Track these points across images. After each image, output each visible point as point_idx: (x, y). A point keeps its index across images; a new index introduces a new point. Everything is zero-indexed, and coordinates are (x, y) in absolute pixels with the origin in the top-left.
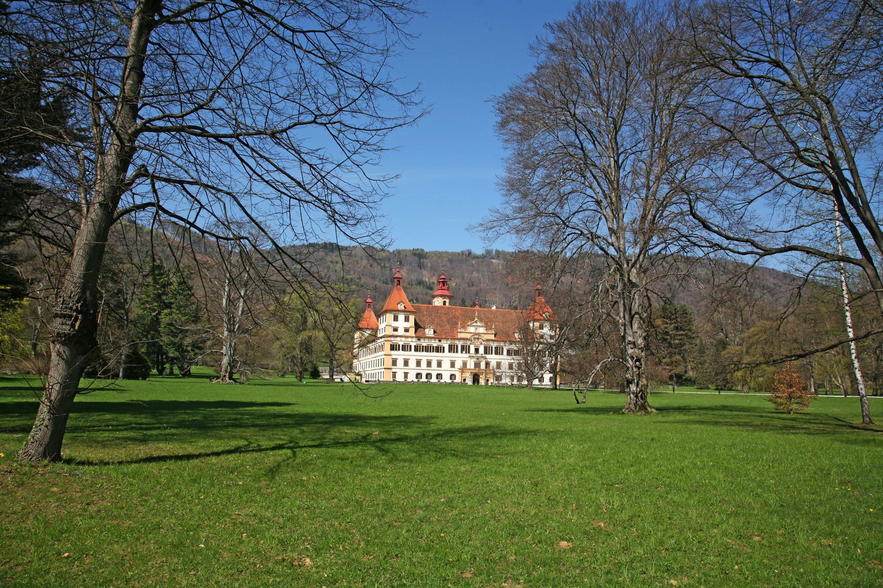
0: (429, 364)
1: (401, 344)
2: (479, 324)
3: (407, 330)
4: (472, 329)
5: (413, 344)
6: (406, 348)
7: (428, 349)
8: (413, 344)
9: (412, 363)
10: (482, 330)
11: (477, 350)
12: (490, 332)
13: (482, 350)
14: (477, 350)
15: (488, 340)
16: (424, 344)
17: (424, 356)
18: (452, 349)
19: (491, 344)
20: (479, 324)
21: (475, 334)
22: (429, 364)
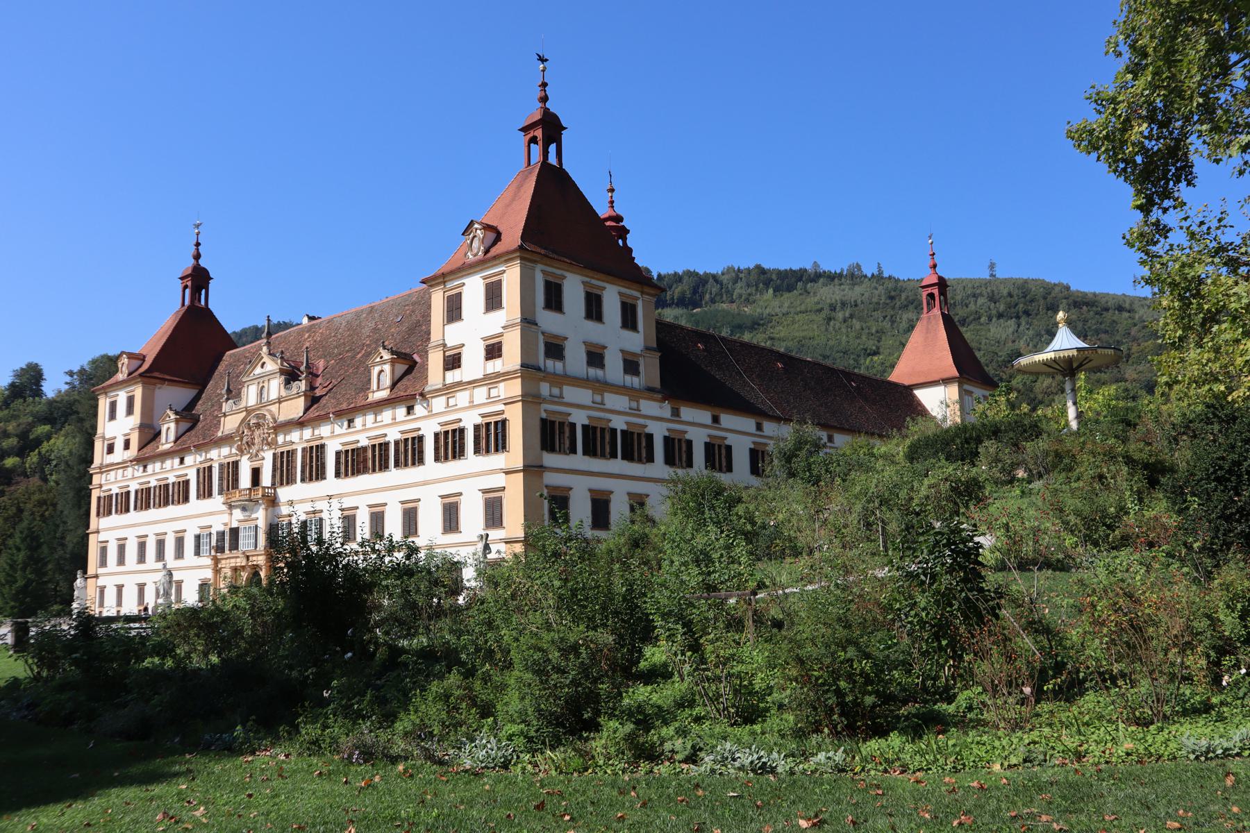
4: (250, 396)
10: (275, 387)
11: (256, 473)
14: (256, 473)
19: (295, 436)
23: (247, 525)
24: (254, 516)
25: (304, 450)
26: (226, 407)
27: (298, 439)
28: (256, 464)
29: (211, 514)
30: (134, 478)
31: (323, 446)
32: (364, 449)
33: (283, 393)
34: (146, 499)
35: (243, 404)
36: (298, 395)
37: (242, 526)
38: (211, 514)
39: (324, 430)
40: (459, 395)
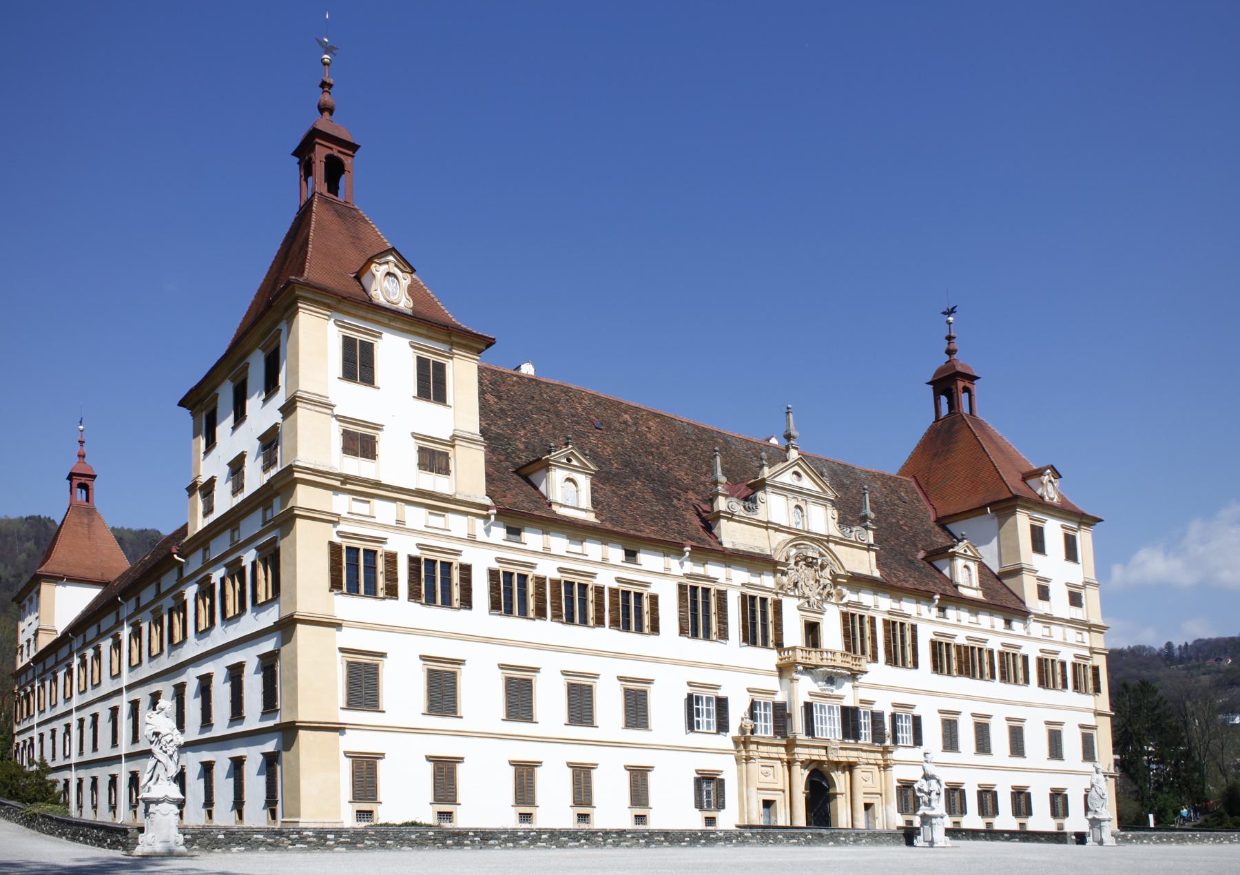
0: (580, 703)
1: (404, 547)
2: (806, 483)
3: (433, 458)
5: (482, 562)
6: (435, 581)
7: (570, 602)
8: (482, 562)
9: (481, 694)
10: (822, 520)
11: (812, 630)
12: (856, 533)
13: (832, 636)
14: (812, 630)
15: (858, 581)
16: (548, 570)
17: (555, 650)
18: (700, 613)
19: (866, 598)
20: (806, 483)
21: (800, 537)
22: (580, 703)
23: (827, 703)
24: (837, 692)
25: (886, 622)
26: (722, 504)
27: (880, 606)
28: (813, 617)
29: (721, 667)
30: (471, 539)
31: (914, 628)
32: (966, 648)
33: (834, 530)
34: (509, 593)
35: (761, 515)
36: (869, 548)
37: (817, 702)
38: (721, 667)
39: (909, 607)
40: (1053, 627)
